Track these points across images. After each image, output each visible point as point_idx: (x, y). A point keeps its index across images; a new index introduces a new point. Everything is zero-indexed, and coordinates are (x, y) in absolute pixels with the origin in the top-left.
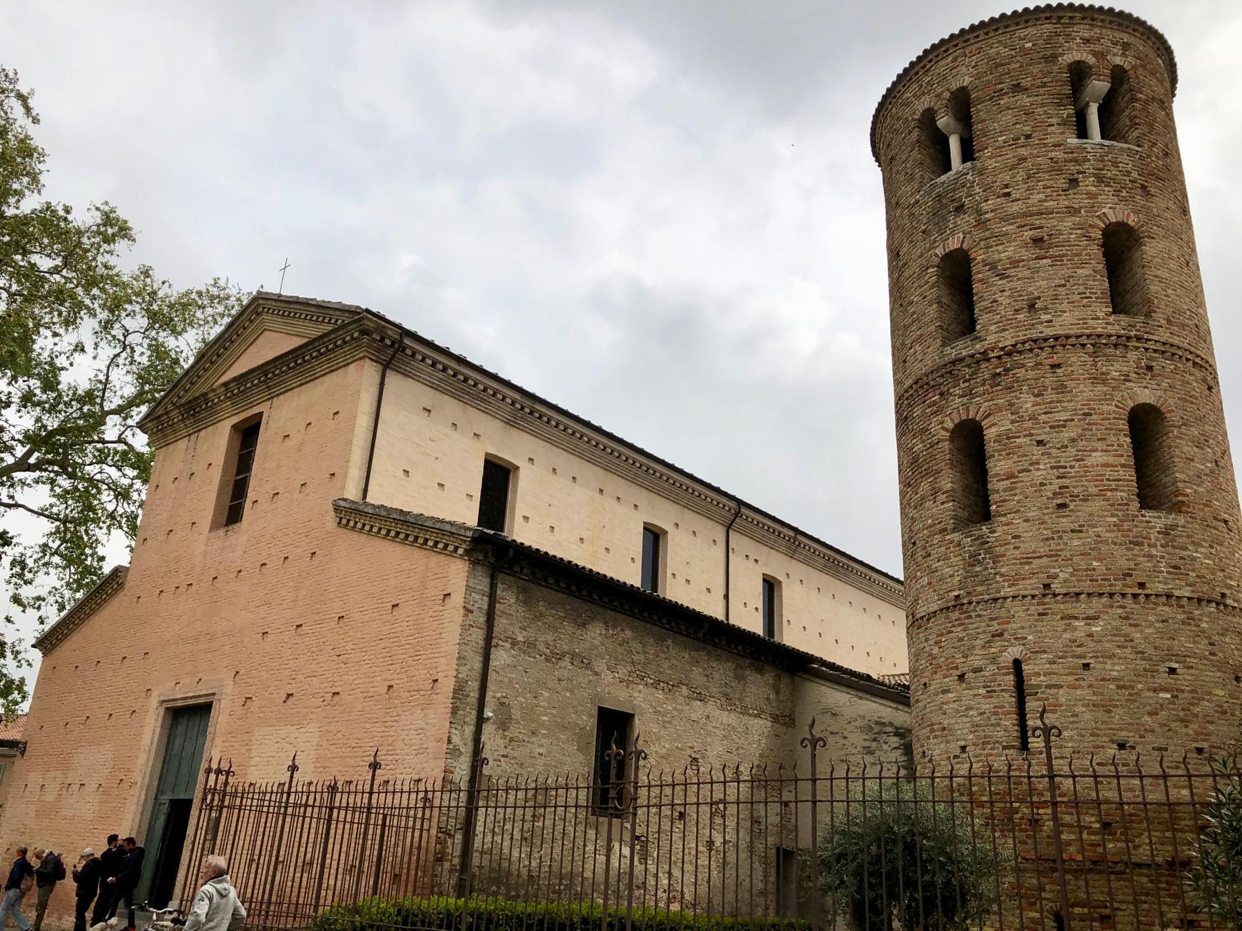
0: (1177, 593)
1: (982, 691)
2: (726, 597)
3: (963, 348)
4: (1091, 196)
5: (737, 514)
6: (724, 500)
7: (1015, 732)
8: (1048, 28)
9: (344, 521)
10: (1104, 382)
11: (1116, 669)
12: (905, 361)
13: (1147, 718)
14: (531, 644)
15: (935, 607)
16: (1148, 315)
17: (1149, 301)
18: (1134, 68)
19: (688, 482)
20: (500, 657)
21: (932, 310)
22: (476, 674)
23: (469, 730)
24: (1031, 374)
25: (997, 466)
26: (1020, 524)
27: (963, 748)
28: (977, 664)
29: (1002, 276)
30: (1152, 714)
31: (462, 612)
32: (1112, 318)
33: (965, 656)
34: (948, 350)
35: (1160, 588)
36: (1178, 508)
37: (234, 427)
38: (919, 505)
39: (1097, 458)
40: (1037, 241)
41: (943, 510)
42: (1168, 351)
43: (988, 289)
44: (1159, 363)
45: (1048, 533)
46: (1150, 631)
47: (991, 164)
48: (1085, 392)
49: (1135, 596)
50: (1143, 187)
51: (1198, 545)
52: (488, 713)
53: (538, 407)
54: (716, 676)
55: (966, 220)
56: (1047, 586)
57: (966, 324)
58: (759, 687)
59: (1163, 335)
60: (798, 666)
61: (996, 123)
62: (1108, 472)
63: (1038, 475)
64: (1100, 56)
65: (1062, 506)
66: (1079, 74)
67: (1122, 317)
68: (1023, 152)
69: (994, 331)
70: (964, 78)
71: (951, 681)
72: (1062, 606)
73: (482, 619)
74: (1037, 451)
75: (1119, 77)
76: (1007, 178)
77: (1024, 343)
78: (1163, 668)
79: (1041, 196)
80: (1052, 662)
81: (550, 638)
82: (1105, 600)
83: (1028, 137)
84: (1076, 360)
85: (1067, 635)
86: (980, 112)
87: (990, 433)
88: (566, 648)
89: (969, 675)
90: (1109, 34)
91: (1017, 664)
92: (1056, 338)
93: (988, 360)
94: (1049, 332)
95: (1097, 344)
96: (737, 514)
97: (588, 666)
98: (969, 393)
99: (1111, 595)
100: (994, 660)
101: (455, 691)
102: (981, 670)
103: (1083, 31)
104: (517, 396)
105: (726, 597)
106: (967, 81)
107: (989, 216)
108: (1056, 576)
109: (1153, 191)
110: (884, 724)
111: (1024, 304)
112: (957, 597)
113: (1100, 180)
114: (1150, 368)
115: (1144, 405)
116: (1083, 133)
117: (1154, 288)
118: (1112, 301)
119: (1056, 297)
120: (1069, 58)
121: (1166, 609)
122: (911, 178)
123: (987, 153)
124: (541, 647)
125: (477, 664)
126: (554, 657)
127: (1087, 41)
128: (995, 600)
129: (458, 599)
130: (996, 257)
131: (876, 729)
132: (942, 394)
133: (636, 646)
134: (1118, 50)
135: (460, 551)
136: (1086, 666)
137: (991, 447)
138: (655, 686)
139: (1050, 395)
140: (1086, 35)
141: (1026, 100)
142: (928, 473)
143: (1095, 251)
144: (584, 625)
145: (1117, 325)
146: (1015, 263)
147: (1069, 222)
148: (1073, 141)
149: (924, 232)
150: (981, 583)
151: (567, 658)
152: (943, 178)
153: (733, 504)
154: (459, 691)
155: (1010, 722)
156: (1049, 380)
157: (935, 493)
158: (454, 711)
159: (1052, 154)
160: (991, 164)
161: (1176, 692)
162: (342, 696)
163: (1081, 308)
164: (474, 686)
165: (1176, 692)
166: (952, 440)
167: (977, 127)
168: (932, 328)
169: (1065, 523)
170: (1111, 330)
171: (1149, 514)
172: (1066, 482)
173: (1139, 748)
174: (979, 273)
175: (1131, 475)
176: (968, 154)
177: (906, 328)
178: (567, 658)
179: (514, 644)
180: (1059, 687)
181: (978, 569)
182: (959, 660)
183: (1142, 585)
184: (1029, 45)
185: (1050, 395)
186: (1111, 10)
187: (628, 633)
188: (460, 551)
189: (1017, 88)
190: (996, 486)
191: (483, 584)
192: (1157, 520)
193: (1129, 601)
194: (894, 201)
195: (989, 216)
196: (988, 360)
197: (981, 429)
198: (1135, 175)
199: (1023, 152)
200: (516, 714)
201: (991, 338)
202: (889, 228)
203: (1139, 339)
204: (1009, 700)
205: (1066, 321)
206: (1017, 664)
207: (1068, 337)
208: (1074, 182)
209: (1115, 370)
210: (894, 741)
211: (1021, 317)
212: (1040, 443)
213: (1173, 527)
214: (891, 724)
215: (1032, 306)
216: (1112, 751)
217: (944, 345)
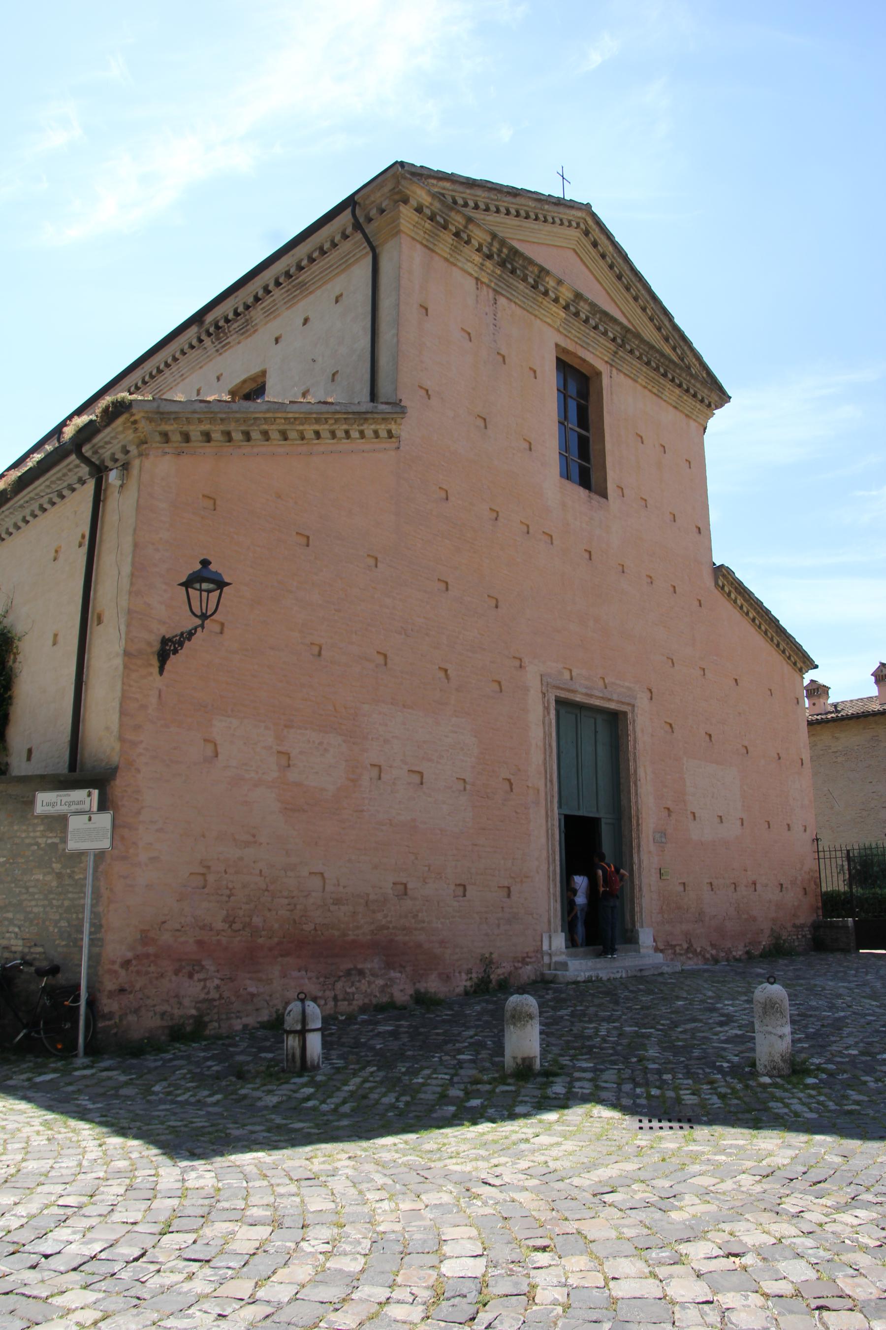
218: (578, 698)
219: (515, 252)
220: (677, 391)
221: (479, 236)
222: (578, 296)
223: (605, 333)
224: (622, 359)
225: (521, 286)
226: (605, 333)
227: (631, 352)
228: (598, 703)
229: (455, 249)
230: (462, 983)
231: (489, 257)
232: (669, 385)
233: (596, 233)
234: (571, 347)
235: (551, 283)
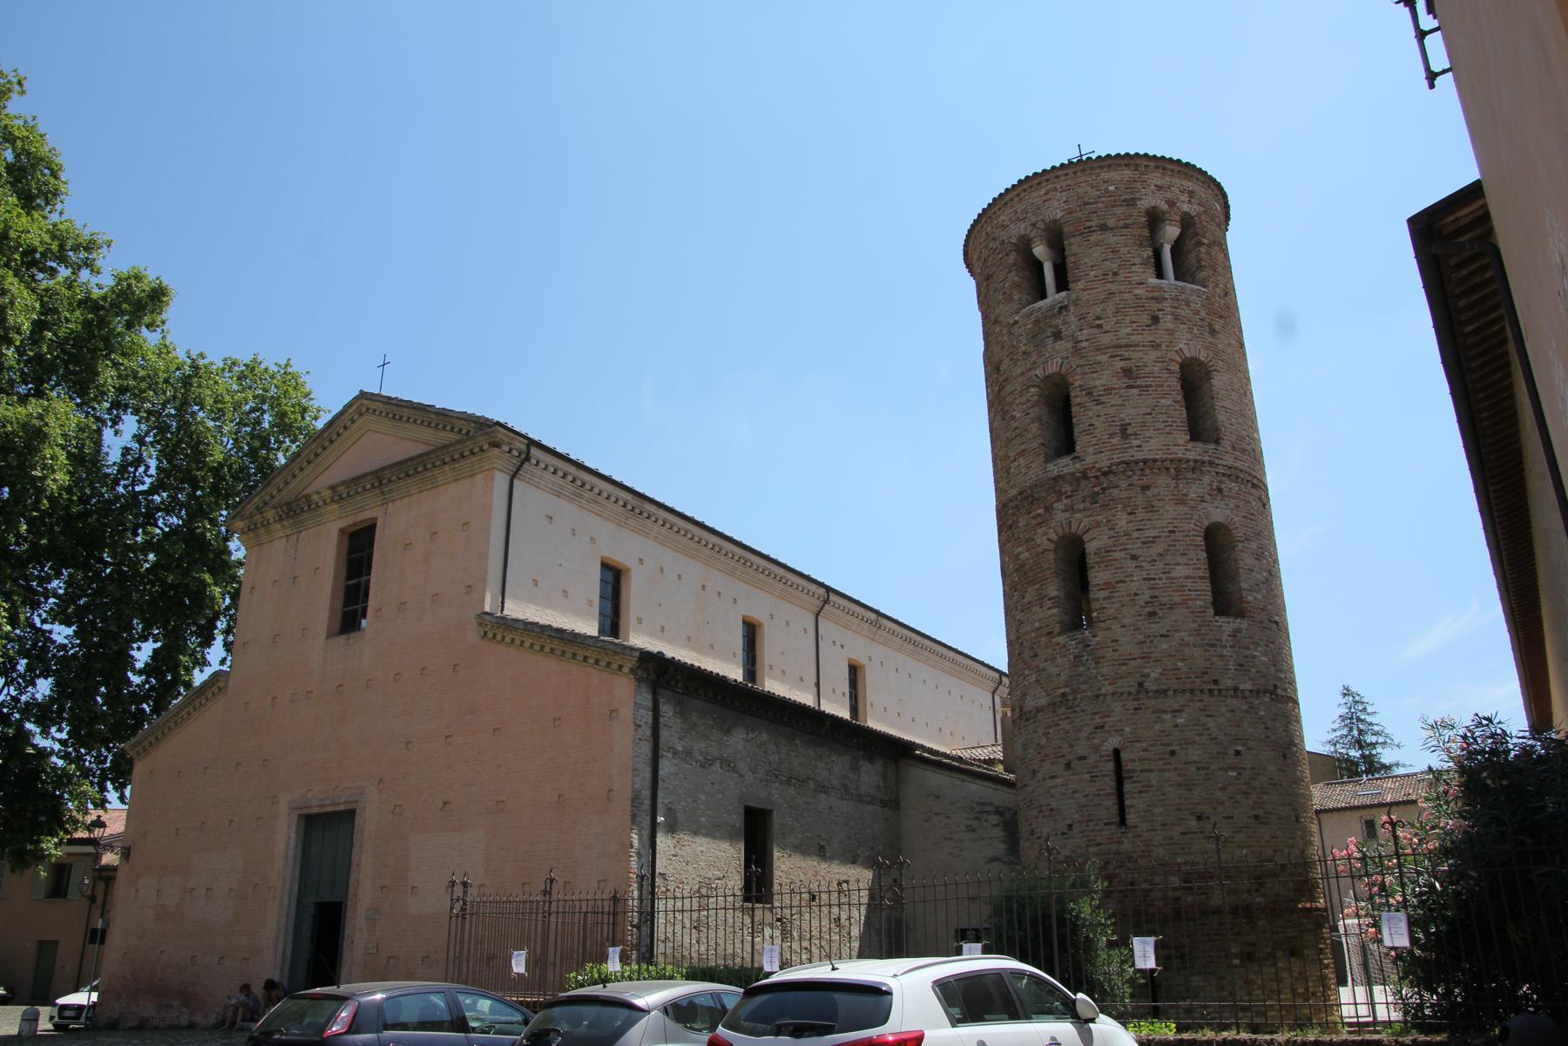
0: (1242, 687)
1: (1086, 777)
2: (818, 685)
3: (1064, 465)
4: (1171, 332)
5: (826, 601)
6: (814, 587)
7: (1115, 810)
8: (1127, 173)
9: (490, 635)
10: (1184, 503)
11: (1195, 754)
13: (1219, 794)
14: (688, 752)
15: (1043, 702)
16: (1217, 441)
17: (1218, 429)
18: (1198, 215)
19: (782, 572)
20: (666, 767)
21: (1034, 429)
22: (648, 783)
23: (646, 833)
24: (1124, 494)
25: (1097, 577)
26: (1118, 628)
27: (1070, 827)
28: (1081, 753)
29: (1098, 402)
30: (1223, 789)
31: (632, 727)
32: (1190, 445)
33: (1071, 746)
34: (1051, 466)
35: (1230, 683)
36: (1241, 614)
37: (342, 531)
38: (1026, 608)
39: (1180, 571)
40: (1127, 372)
41: (1051, 615)
42: (1234, 474)
43: (1085, 416)
44: (1229, 486)
45: (1140, 637)
46: (1221, 720)
47: (1085, 296)
48: (1170, 512)
49: (1211, 691)
50: (1210, 325)
51: (1256, 644)
52: (660, 819)
53: (647, 506)
54: (836, 769)
55: (1062, 346)
56: (1141, 685)
57: (1065, 443)
58: (870, 775)
59: (1229, 460)
60: (898, 752)
61: (1086, 257)
62: (1189, 583)
63: (1133, 587)
64: (1171, 203)
65: (1152, 614)
66: (1154, 220)
67: (1200, 445)
68: (1113, 287)
69: (1092, 452)
70: (1056, 211)
71: (1058, 768)
72: (1153, 702)
73: (649, 733)
74: (1131, 564)
75: (1187, 223)
76: (1098, 310)
77: (1118, 464)
78: (1231, 752)
79: (1128, 330)
80: (1145, 750)
81: (702, 745)
82: (1188, 696)
83: (1115, 274)
84: (1163, 482)
85: (1158, 727)
86: (1073, 246)
87: (1091, 547)
88: (716, 754)
89: (1075, 763)
90: (1178, 182)
91: (1117, 752)
92: (1145, 462)
94: (1139, 456)
95: (1180, 469)
96: (826, 601)
97: (734, 770)
98: (1069, 509)
99: (1192, 691)
100: (1097, 748)
101: (633, 800)
102: (1084, 758)
103: (1156, 178)
104: (628, 496)
105: (818, 685)
106: (1059, 214)
107: (1084, 344)
108: (1148, 675)
109: (1217, 327)
112: (1064, 695)
113: (1176, 317)
114: (1220, 490)
115: (1216, 524)
116: (1160, 274)
117: (1221, 417)
118: (1190, 429)
119: (1143, 425)
120: (1146, 202)
121: (1235, 701)
122: (1009, 299)
123: (1080, 285)
124: (696, 755)
125: (647, 773)
126: (707, 763)
127: (1159, 188)
128: (1097, 696)
129: (627, 713)
130: (1091, 383)
131: (978, 809)
132: (1047, 509)
133: (772, 747)
134: (1185, 197)
135: (626, 670)
136: (1173, 753)
137: (1091, 559)
138: (788, 782)
139: (1140, 515)
140: (1159, 183)
141: (1112, 239)
142: (1033, 582)
143: (1175, 383)
144: (728, 732)
145: (1195, 451)
146: (1109, 391)
147: (1153, 355)
148: (1153, 281)
151: (718, 764)
152: (1041, 303)
153: (822, 591)
154: (635, 799)
155: (1110, 803)
156: (1140, 500)
157: (1041, 598)
158: (634, 817)
159: (1136, 291)
160: (1085, 296)
161: (1240, 770)
163: (1166, 438)
164: (646, 793)
165: (1240, 770)
166: (1056, 550)
167: (1070, 260)
168: (1035, 445)
169: (1156, 628)
170: (1191, 455)
171: (1221, 619)
172: (1156, 593)
173: (1213, 819)
174: (1077, 398)
175: (1206, 585)
176: (1062, 284)
177: (1009, 441)
178: (718, 764)
179: (675, 753)
180: (1150, 771)
181: (1081, 669)
182: (1066, 750)
183: (1216, 682)
184: (1112, 188)
186: (1179, 161)
187: (765, 736)
188: (626, 670)
189: (1104, 228)
190: (1095, 594)
191: (646, 699)
192: (1227, 624)
193: (1206, 697)
194: (992, 317)
195: (1084, 344)
197: (1082, 542)
198: (1203, 314)
199: (1113, 287)
200: (681, 816)
201: (1090, 459)
202: (985, 338)
203: (1211, 463)
204: (1109, 783)
205: (1152, 446)
206: (1117, 752)
207: (1155, 461)
208: (1155, 319)
209: (1193, 492)
210: (995, 819)
211: (1114, 441)
212: (1134, 557)
213: (1238, 631)
214: (991, 804)
215: (1124, 434)
216: (1193, 823)
217: (1047, 461)
218: (315, 811)
219: (288, 504)
221: (270, 514)
222: (333, 488)
223: (365, 489)
224: (391, 491)
225: (305, 516)
226: (365, 489)
227: (390, 481)
228: (330, 809)
229: (269, 532)
230: (212, 1019)
231: (281, 519)
232: (436, 471)
233: (373, 405)
234: (351, 521)
235: (315, 497)
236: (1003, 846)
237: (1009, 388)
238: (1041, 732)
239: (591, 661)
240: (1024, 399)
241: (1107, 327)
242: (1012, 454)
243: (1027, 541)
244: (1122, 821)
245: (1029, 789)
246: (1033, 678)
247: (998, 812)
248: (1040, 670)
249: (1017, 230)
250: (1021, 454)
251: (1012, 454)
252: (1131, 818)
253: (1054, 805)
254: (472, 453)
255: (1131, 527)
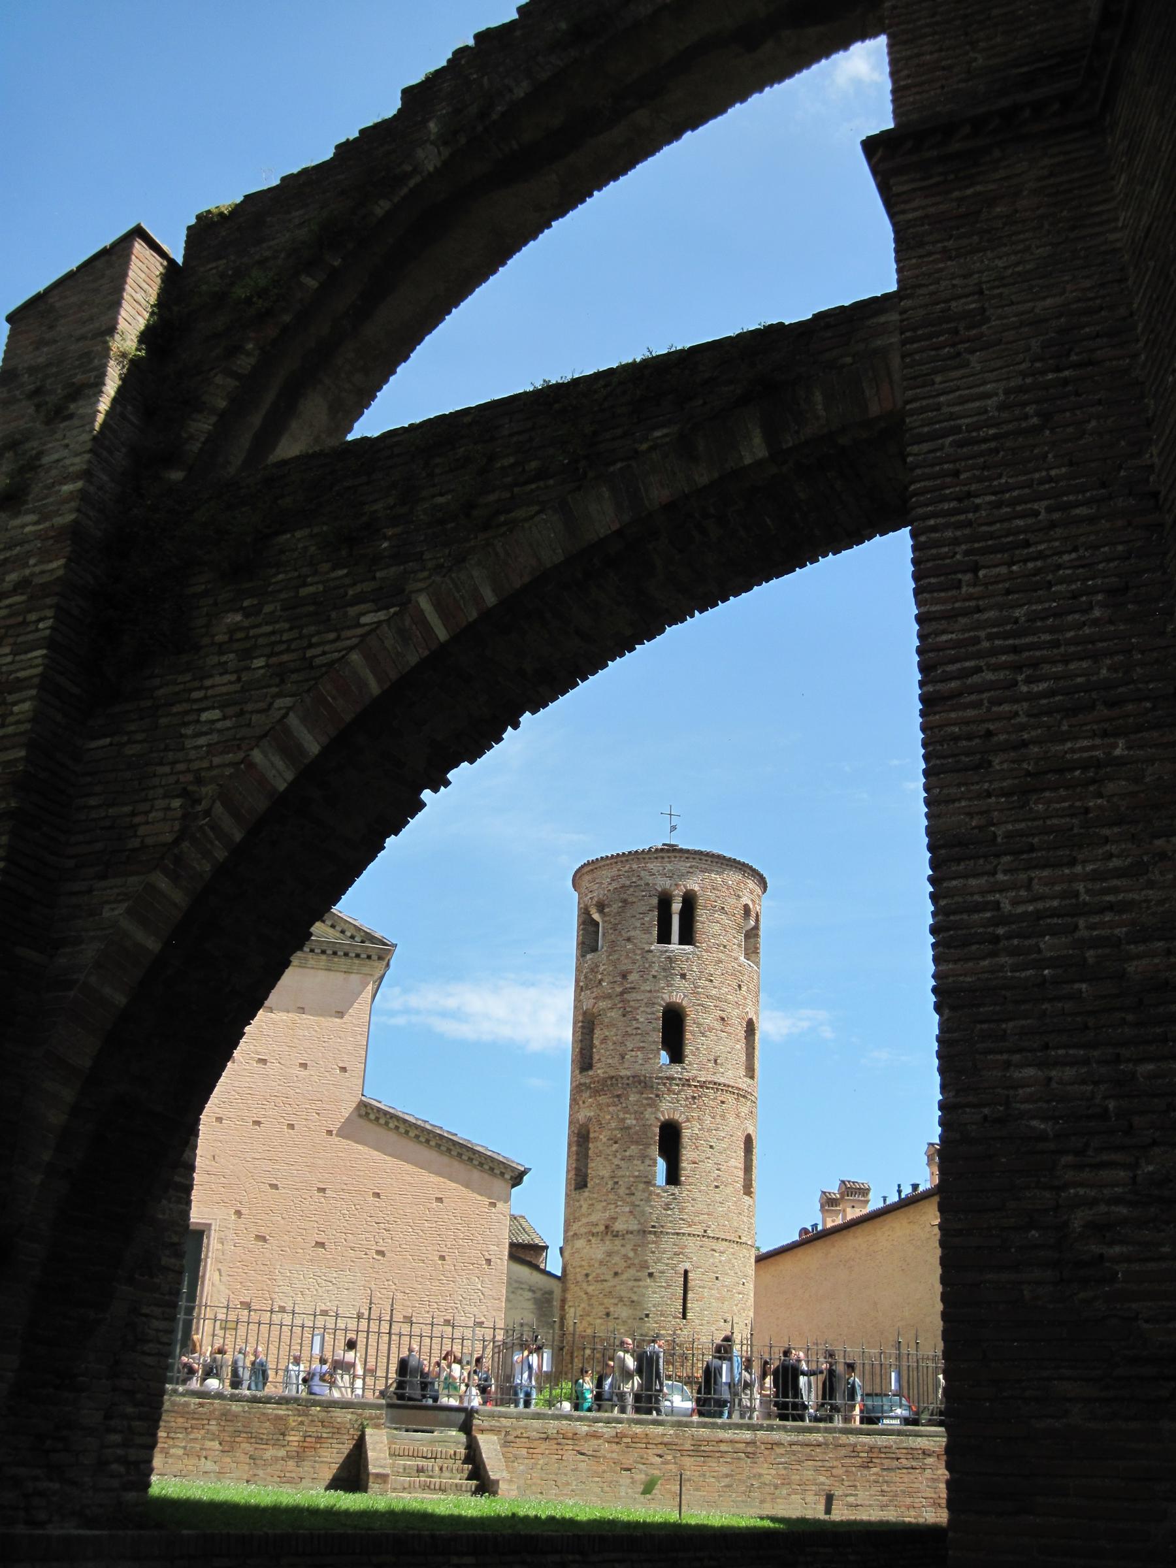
12: (623, 1058)
27: (647, 1316)
83: (725, 947)
84: (730, 1099)
87: (686, 1133)
91: (686, 1272)
93: (690, 1086)
94: (722, 1080)
106: (696, 888)
110: (521, 1283)
111: (712, 1058)
122: (647, 931)
128: (678, 1234)
131: (516, 1285)
136: (717, 1278)
139: (718, 1120)
142: (637, 1143)
149: (654, 977)
150: (671, 1222)
162: (254, 1231)
174: (690, 1028)
185: (718, 1120)
188: (507, 1176)
196: (690, 1086)
206: (686, 1272)
215: (716, 1061)
220: (324, 957)
232: (310, 955)
236: (531, 1316)
237: (634, 996)
238: (629, 1247)
239: (475, 1162)
240: (649, 1010)
241: (716, 983)
242: (630, 1046)
243: (636, 1112)
244: (684, 1317)
245: (609, 1284)
246: (627, 1209)
247: (530, 1290)
248: (634, 1205)
249: (662, 883)
250: (640, 1049)
251: (630, 1046)
252: (689, 1315)
253: (635, 1298)
254: (358, 956)
255: (713, 1126)
